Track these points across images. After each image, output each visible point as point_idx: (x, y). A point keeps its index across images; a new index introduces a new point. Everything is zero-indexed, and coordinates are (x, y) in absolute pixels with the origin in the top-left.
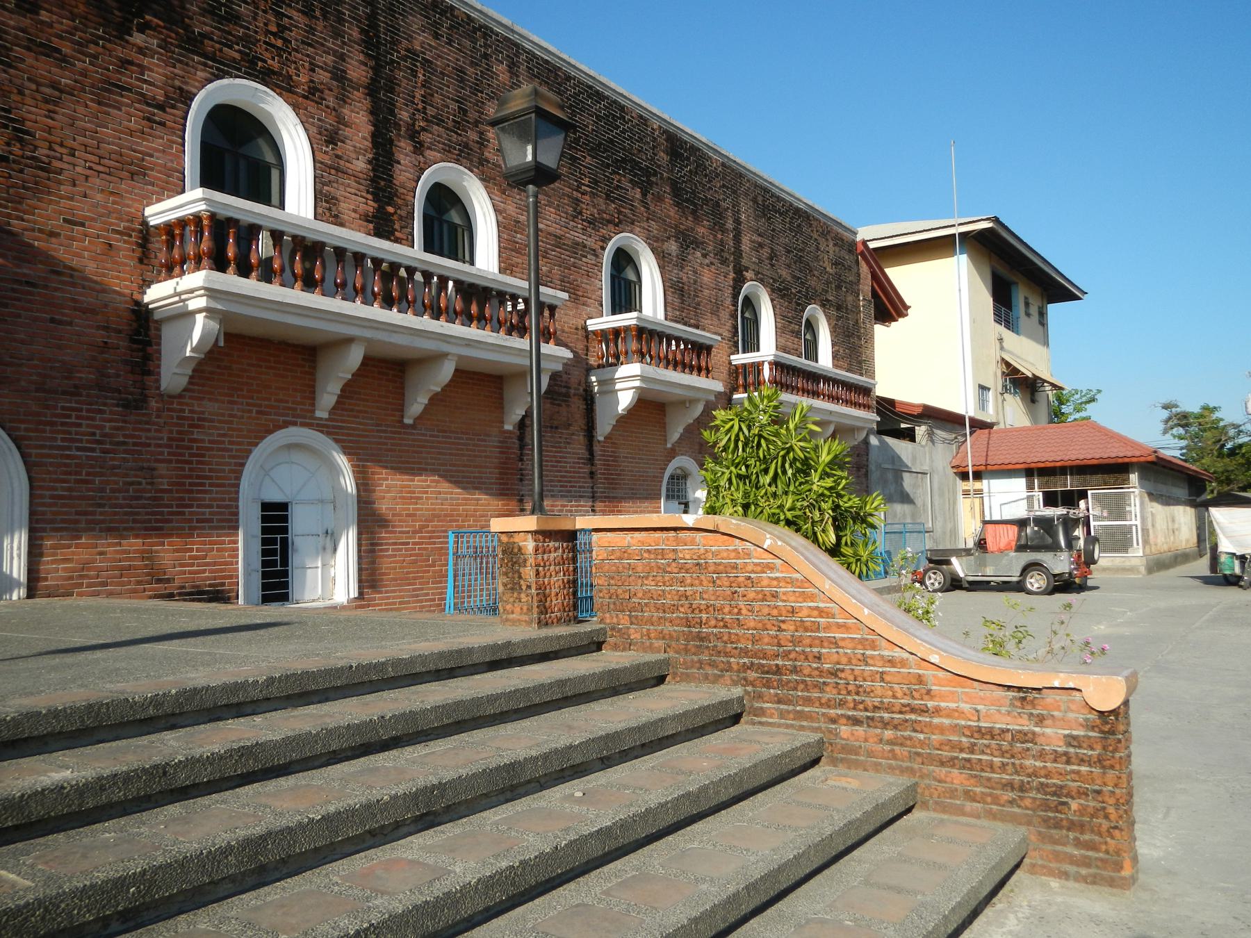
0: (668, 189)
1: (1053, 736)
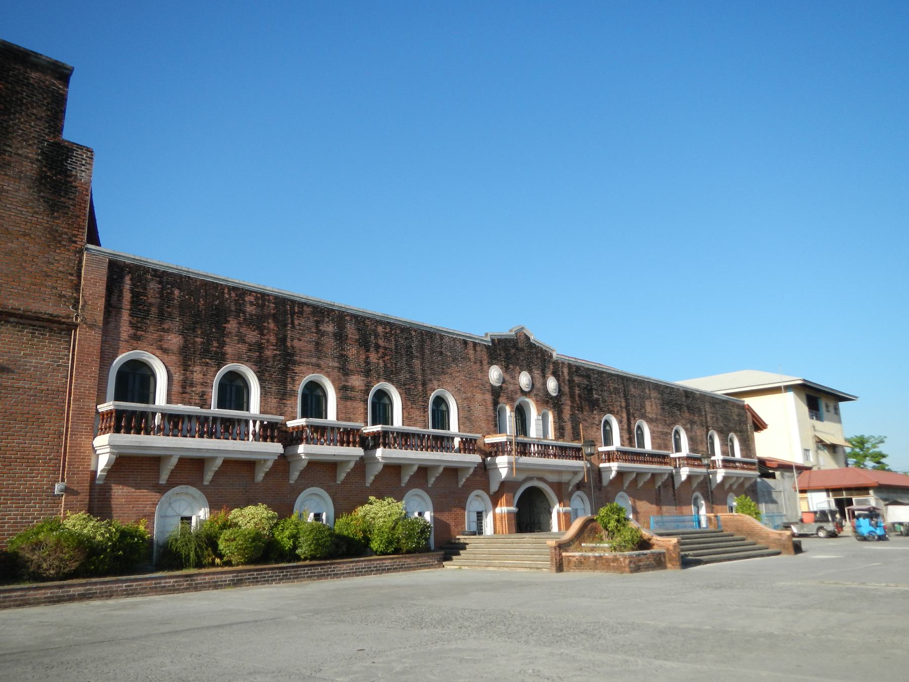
0: (686, 408)
1: (783, 538)
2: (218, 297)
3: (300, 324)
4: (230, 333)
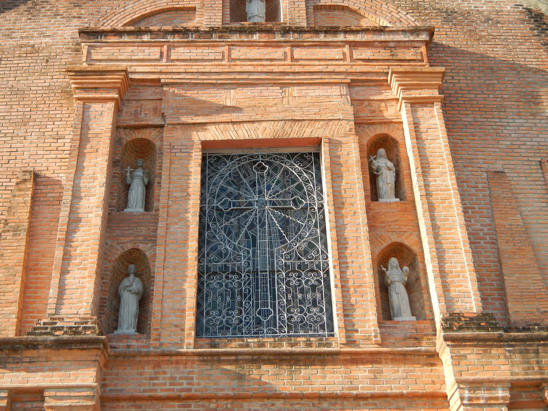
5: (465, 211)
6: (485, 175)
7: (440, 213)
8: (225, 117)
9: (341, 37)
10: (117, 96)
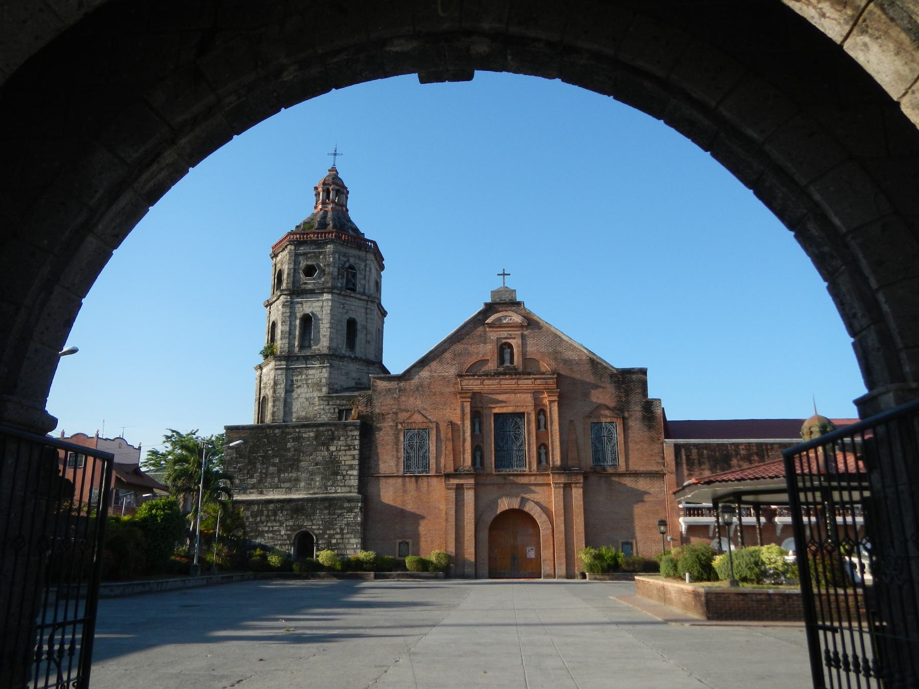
2: (725, 450)
3: (772, 455)
4: (734, 465)
5: (560, 436)
6: (568, 422)
7: (554, 438)
8: (499, 405)
9: (532, 376)
10: (470, 400)
